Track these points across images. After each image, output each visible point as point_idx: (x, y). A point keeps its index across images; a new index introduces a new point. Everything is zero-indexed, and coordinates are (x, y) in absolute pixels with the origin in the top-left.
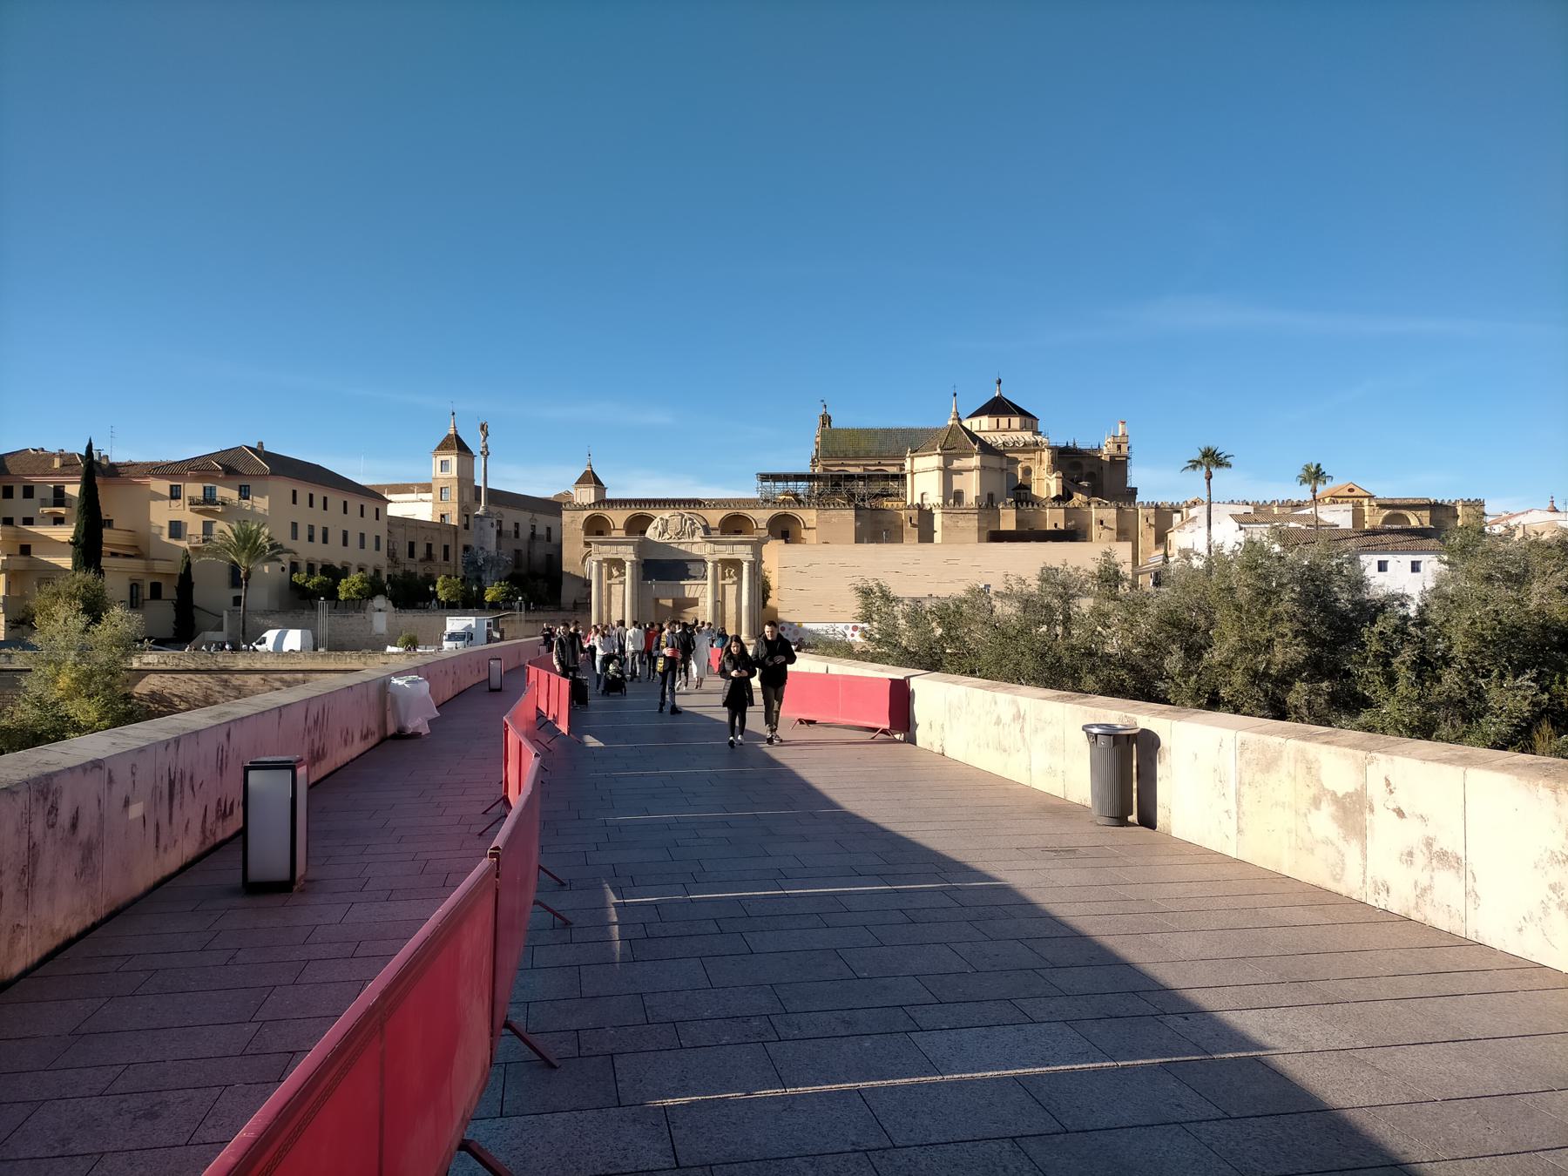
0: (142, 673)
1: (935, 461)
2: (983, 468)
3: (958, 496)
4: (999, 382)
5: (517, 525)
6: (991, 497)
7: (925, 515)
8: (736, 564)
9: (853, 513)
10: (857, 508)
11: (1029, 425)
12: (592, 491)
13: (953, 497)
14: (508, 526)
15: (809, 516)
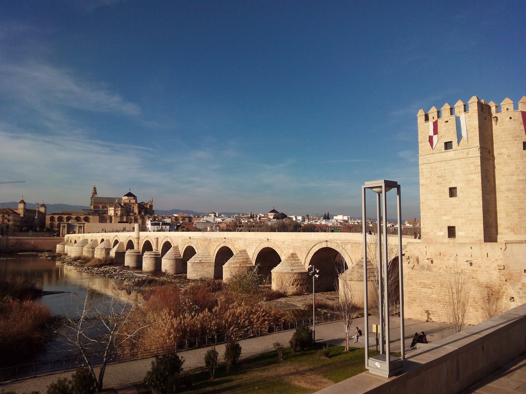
0: (10, 239)
1: (113, 208)
2: (121, 210)
3: (117, 214)
4: (130, 190)
5: (31, 216)
6: (122, 214)
7: (111, 217)
8: (81, 226)
9: (98, 217)
10: (99, 216)
11: (135, 198)
12: (44, 208)
13: (116, 214)
14: (30, 216)
15: (91, 217)
